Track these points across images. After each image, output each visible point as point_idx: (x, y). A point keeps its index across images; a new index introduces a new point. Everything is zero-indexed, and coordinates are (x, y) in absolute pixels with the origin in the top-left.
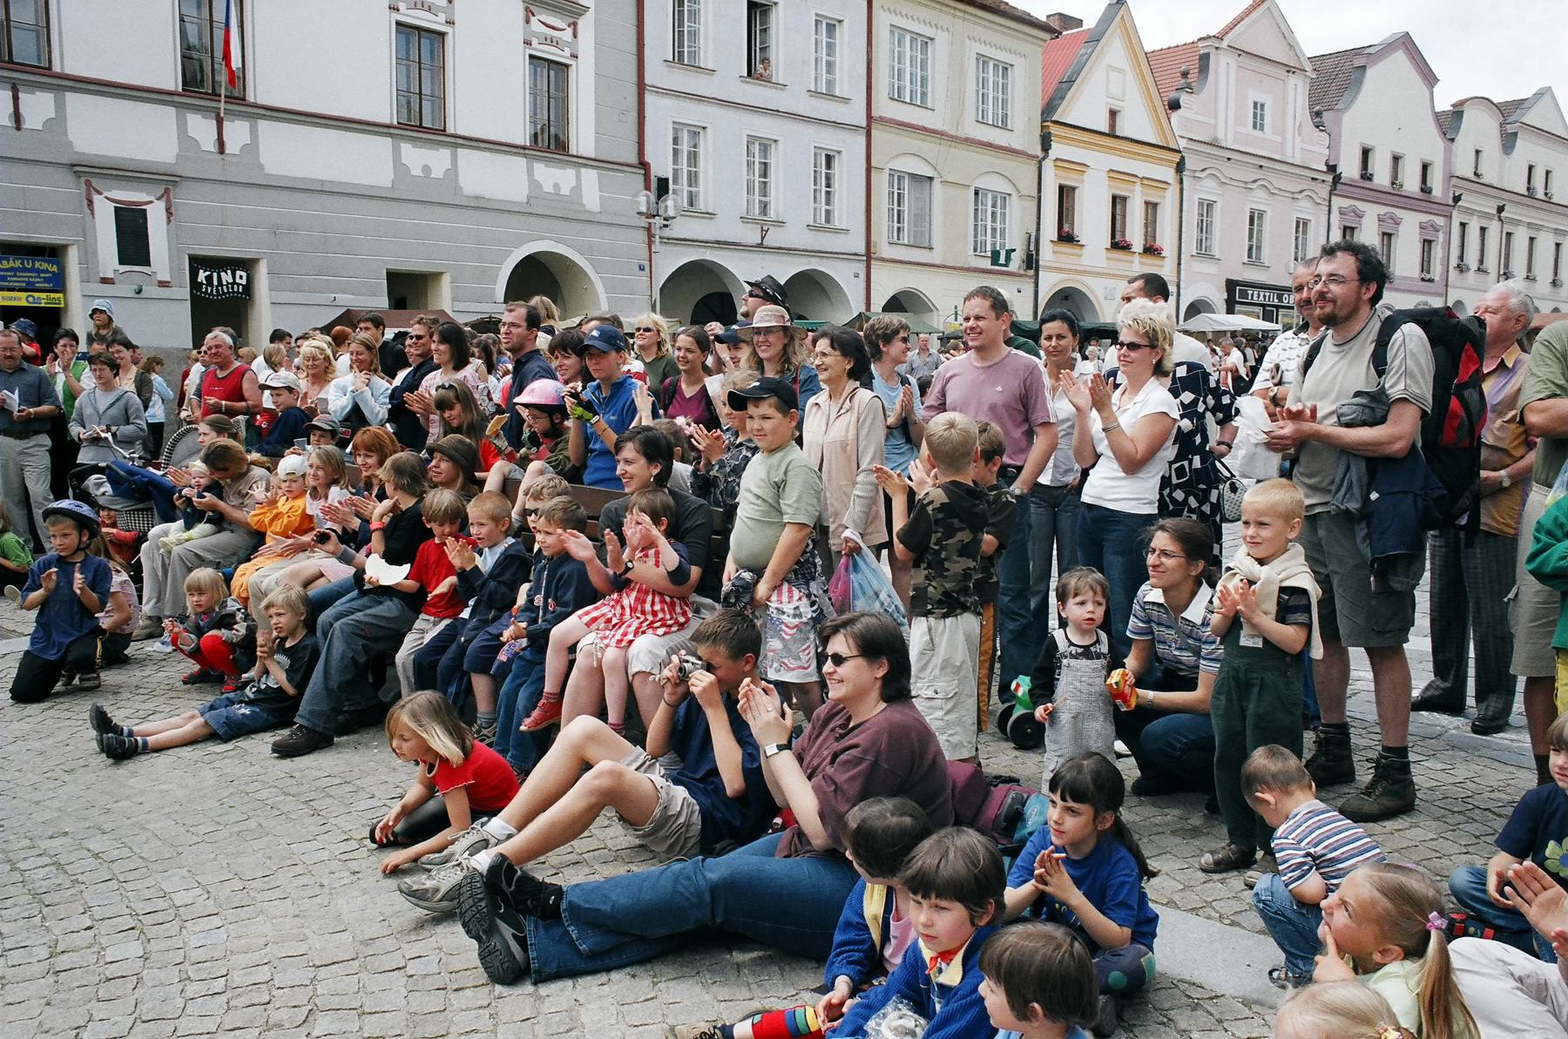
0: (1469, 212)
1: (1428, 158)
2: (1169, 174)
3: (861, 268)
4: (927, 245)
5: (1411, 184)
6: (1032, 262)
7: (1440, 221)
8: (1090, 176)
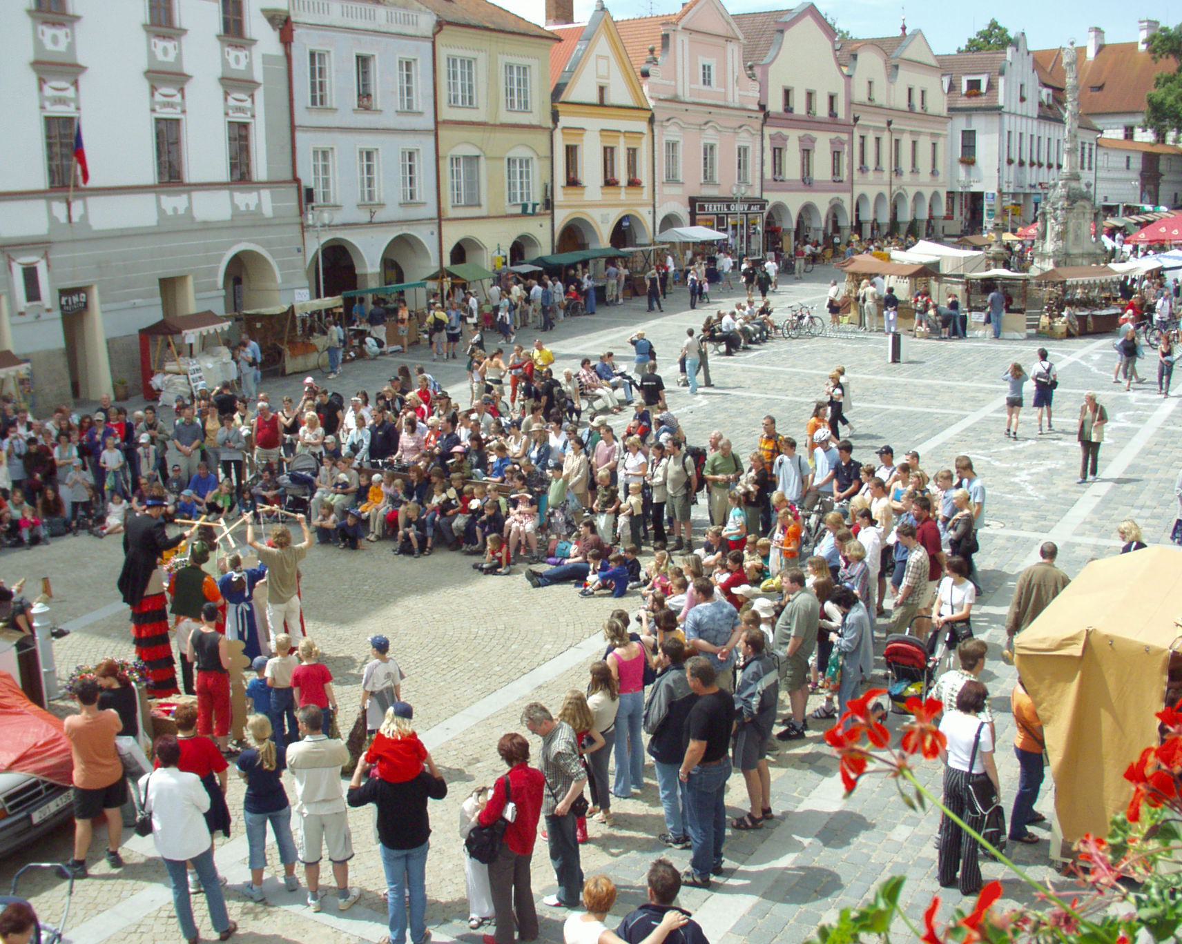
0: (867, 127)
1: (833, 91)
2: (643, 126)
3: (435, 228)
4: (476, 202)
5: (822, 111)
6: (549, 204)
7: (845, 137)
8: (587, 136)
